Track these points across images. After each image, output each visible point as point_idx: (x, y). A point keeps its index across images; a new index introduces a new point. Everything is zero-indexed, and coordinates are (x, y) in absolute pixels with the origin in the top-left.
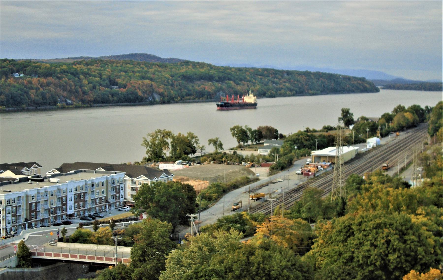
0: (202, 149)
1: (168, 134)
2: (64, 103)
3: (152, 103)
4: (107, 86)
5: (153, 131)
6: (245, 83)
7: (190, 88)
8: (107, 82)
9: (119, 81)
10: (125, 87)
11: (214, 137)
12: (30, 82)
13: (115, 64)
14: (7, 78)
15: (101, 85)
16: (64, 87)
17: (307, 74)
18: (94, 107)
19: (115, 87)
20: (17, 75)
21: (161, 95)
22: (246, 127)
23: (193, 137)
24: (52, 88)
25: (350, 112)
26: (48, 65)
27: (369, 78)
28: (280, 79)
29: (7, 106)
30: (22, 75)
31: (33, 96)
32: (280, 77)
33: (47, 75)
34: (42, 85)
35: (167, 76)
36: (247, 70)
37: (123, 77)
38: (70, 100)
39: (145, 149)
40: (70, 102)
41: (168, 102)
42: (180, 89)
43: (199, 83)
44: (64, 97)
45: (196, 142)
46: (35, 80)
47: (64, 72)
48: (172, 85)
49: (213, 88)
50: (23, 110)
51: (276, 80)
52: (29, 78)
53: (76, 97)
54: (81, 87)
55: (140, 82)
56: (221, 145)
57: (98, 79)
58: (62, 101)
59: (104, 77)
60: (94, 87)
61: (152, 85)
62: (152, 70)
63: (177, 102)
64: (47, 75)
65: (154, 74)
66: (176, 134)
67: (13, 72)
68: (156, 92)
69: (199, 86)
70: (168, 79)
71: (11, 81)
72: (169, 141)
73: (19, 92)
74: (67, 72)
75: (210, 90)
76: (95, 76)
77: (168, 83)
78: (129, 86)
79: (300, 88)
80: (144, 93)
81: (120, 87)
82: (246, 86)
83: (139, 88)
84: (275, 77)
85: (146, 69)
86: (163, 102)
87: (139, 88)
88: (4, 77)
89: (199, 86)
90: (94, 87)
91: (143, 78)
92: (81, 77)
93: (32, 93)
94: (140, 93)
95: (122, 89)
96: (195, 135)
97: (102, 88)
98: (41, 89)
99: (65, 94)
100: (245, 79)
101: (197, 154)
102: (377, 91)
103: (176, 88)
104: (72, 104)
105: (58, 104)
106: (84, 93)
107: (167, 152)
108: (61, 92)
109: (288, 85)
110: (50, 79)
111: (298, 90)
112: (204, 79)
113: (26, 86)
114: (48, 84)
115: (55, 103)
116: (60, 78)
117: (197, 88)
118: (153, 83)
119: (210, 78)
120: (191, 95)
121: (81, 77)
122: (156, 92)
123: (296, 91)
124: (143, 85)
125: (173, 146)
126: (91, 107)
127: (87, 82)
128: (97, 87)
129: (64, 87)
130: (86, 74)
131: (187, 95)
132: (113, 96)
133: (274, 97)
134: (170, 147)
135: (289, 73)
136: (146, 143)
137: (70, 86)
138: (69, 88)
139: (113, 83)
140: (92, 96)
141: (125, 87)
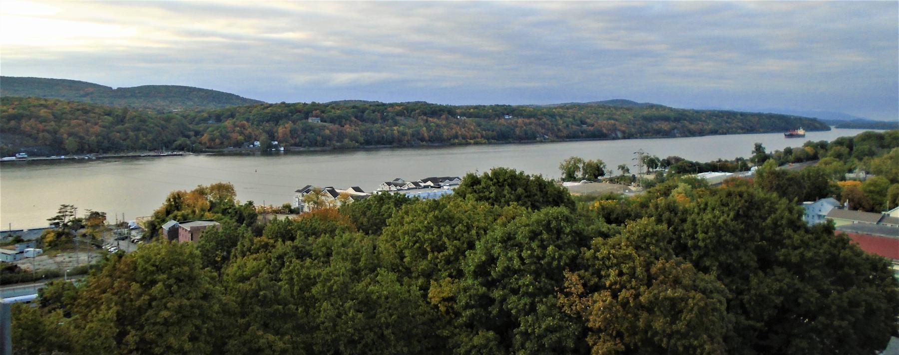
0: (611, 172)
1: (580, 161)
2: (542, 138)
3: (616, 138)
4: (578, 125)
5: (568, 158)
6: (700, 123)
7: (649, 126)
8: (579, 122)
9: (588, 121)
10: (593, 125)
11: (621, 164)
12: (517, 122)
13: (589, 108)
14: (499, 119)
15: (572, 124)
16: (543, 126)
17: (760, 115)
18: (566, 141)
19: (585, 126)
20: (507, 117)
21: (623, 132)
22: (654, 156)
23: (601, 164)
24: (533, 127)
25: (763, 146)
26: (532, 109)
27: (820, 117)
28: (733, 120)
29: (497, 140)
30: (510, 117)
31: (518, 133)
32: (733, 118)
33: (529, 117)
34: (526, 124)
35: (630, 117)
36: (703, 112)
37: (592, 118)
38: (547, 135)
39: (561, 171)
40: (547, 137)
41: (629, 138)
42: (640, 128)
43: (657, 122)
44: (542, 133)
45: (604, 166)
46: (520, 120)
47: (545, 114)
48: (634, 124)
49: (669, 126)
50: (510, 143)
51: (729, 120)
52: (516, 119)
53: (552, 134)
54: (556, 125)
55: (605, 122)
56: (628, 170)
57: (571, 120)
58: (540, 136)
59: (576, 118)
60: (567, 126)
61: (615, 124)
62: (618, 113)
63: (636, 138)
64: (677, 120)
65: (619, 115)
66: (587, 161)
67: (504, 114)
68: (619, 130)
69: (657, 125)
70: (630, 119)
71: (502, 121)
72: (581, 166)
73: (507, 129)
74: (547, 114)
75: (666, 128)
76: (569, 117)
77: (630, 122)
78: (596, 125)
79: (751, 127)
80: (609, 130)
81: (588, 126)
82: (700, 125)
83: (604, 127)
84: (728, 118)
85: (614, 111)
86: (624, 138)
87: (604, 127)
88: (497, 118)
89: (657, 125)
90: (567, 126)
91: (609, 119)
92: (558, 118)
93: (518, 131)
94: (605, 131)
95: (590, 127)
96: (603, 161)
97: (573, 126)
98: (525, 127)
99: (543, 131)
100: (700, 120)
101: (605, 177)
102: (829, 129)
103: (637, 127)
104: (548, 139)
105: (538, 139)
106: (559, 130)
107: (579, 174)
108: (539, 129)
109: (740, 124)
110: (532, 120)
111: (749, 129)
112: (662, 120)
113: (513, 125)
114: (530, 124)
115: (535, 138)
116: (540, 119)
117: (655, 127)
118: (617, 123)
119: (666, 119)
120: (649, 132)
121: (558, 118)
122: (619, 130)
123: (748, 130)
124: (608, 124)
125: (584, 169)
126: (564, 141)
127: (561, 122)
128: (570, 125)
129: (543, 126)
130: (561, 116)
131: (646, 132)
132: (582, 133)
133: (726, 134)
134: (581, 169)
135: (742, 114)
136: (562, 167)
137: (548, 124)
138: (546, 127)
139: (583, 122)
140: (565, 132)
141: (593, 125)
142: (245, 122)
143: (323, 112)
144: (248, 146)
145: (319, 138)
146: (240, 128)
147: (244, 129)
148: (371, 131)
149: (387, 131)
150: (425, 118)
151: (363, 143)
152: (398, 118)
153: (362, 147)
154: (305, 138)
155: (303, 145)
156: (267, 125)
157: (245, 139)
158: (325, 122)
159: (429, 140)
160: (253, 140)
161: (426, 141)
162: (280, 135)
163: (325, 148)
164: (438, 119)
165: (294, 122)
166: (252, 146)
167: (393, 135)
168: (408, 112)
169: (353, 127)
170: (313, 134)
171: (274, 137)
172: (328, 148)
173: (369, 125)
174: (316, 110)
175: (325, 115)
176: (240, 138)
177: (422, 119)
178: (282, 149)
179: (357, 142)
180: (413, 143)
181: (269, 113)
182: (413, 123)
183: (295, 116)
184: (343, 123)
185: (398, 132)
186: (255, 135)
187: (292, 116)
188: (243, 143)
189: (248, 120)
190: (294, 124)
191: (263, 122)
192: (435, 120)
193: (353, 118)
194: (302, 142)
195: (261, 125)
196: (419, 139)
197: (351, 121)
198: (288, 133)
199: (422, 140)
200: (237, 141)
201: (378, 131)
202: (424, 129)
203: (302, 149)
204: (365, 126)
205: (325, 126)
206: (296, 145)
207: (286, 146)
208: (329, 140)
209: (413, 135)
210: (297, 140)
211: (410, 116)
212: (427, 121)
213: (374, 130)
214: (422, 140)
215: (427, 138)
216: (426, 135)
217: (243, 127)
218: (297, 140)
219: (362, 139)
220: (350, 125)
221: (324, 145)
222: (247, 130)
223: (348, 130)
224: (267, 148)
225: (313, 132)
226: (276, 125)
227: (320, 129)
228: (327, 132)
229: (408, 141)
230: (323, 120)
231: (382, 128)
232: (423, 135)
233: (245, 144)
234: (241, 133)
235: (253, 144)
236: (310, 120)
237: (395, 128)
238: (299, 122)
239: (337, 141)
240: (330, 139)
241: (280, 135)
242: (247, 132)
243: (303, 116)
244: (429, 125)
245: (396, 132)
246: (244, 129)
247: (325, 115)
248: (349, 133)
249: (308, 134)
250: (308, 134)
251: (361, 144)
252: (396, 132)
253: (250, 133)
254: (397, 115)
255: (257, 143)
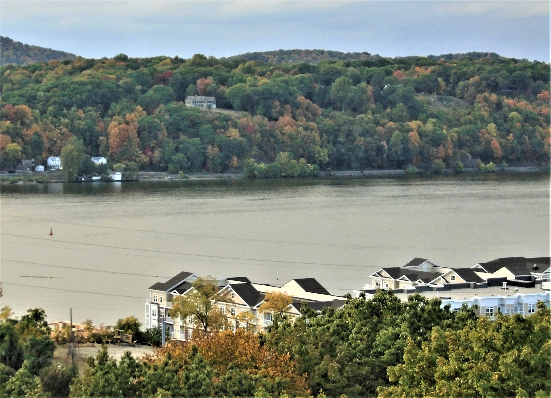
142: (25, 107)
143: (223, 82)
144: (33, 169)
145: (212, 150)
146: (13, 121)
147: (23, 123)
148: (349, 134)
149: (391, 131)
150: (494, 97)
151: (328, 164)
152: (420, 98)
153: (322, 174)
154: (177, 150)
155: (170, 166)
156: (81, 113)
157: (24, 152)
158: (229, 106)
159: (505, 158)
160: (44, 155)
161: (494, 160)
162: (113, 141)
163: (225, 176)
164: (528, 99)
165: (149, 108)
166: (41, 168)
167: (405, 141)
168: (447, 80)
169: (302, 121)
170: (197, 140)
171: (97, 146)
172: (233, 176)
173: (342, 116)
174: (205, 75)
175: (227, 90)
176: (14, 147)
177: (486, 100)
178: (118, 176)
179: (311, 159)
180: (461, 164)
181: (84, 84)
182: (462, 111)
183: (151, 92)
184: (274, 112)
185: (421, 135)
186: (50, 140)
187: (144, 92)
188: (19, 161)
189: (32, 100)
190: (149, 114)
191: (69, 107)
192: (523, 104)
193: (301, 98)
194: (169, 161)
195: (65, 116)
196: (475, 155)
197: (297, 106)
198: (133, 134)
199: (487, 156)
200: (7, 154)
201: (366, 133)
202: (492, 127)
203: (167, 178)
204: (332, 118)
205: (227, 119)
206: (151, 166)
207: (125, 170)
208: (239, 157)
209: (460, 144)
210: (157, 154)
211: (452, 93)
212: (499, 106)
213: (357, 129)
214: (487, 156)
215: (499, 153)
216: (495, 143)
217: (19, 118)
218: (157, 154)
219: (323, 154)
220: (294, 117)
221: (225, 168)
222: (29, 126)
223: (287, 129)
224: (81, 173)
225: (197, 136)
226: (103, 115)
227: (215, 128)
228: (234, 133)
229: (446, 160)
230: (224, 104)
231: (377, 123)
232: (489, 143)
233: (24, 162)
234: (15, 135)
235: (45, 164)
236: (189, 103)
237: (413, 124)
238: (162, 107)
239: (259, 159)
240: (241, 153)
241: (113, 141)
242: (29, 133)
243: (170, 90)
244: (506, 119)
245: (414, 136)
246: (23, 123)
247: (227, 90)
248: (292, 137)
249: (183, 137)
250: (183, 137)
251: (322, 166)
252: (414, 136)
253: (36, 133)
254: (418, 90)
255: (55, 162)
